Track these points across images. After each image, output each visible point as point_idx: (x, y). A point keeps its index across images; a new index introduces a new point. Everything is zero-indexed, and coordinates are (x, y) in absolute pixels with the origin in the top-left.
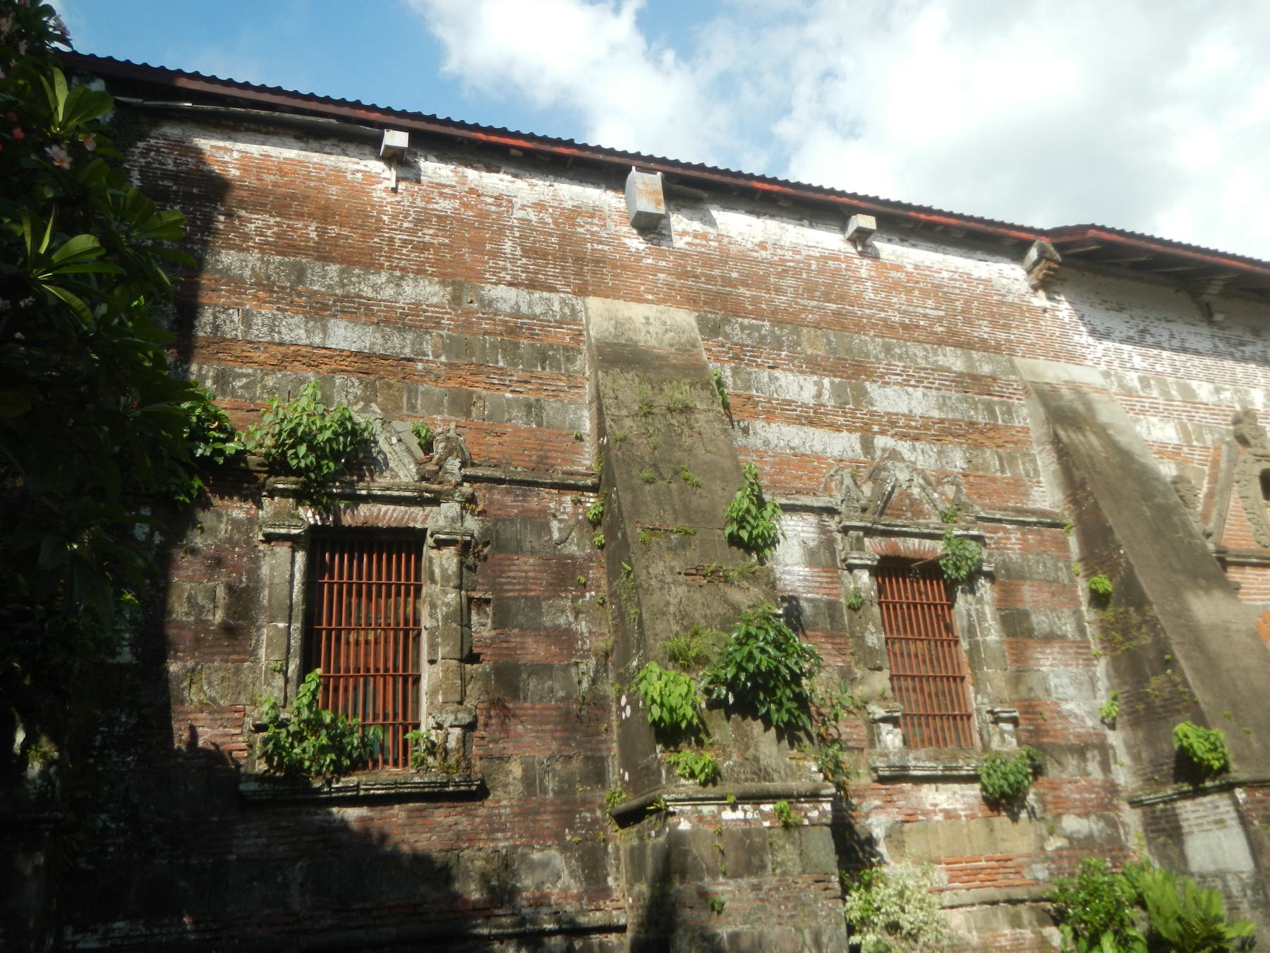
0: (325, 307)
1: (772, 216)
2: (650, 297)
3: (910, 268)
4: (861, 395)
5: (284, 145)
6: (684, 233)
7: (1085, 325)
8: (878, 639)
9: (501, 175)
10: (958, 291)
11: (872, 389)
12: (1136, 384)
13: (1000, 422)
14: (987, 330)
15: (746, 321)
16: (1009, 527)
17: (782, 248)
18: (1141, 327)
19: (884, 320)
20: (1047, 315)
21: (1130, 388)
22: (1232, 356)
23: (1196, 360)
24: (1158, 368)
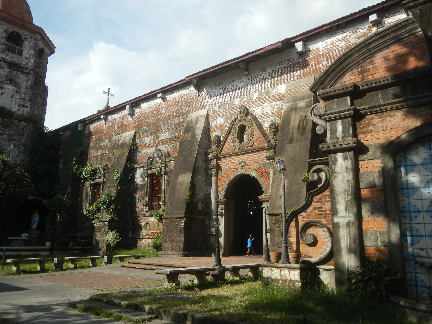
1: (150, 101)
3: (172, 100)
4: (157, 137)
6: (137, 112)
8: (147, 191)
9: (116, 114)
10: (180, 101)
11: (159, 135)
12: (217, 108)
14: (184, 109)
15: (142, 128)
18: (224, 88)
19: (165, 117)
21: (215, 111)
22: (252, 84)
23: (238, 91)
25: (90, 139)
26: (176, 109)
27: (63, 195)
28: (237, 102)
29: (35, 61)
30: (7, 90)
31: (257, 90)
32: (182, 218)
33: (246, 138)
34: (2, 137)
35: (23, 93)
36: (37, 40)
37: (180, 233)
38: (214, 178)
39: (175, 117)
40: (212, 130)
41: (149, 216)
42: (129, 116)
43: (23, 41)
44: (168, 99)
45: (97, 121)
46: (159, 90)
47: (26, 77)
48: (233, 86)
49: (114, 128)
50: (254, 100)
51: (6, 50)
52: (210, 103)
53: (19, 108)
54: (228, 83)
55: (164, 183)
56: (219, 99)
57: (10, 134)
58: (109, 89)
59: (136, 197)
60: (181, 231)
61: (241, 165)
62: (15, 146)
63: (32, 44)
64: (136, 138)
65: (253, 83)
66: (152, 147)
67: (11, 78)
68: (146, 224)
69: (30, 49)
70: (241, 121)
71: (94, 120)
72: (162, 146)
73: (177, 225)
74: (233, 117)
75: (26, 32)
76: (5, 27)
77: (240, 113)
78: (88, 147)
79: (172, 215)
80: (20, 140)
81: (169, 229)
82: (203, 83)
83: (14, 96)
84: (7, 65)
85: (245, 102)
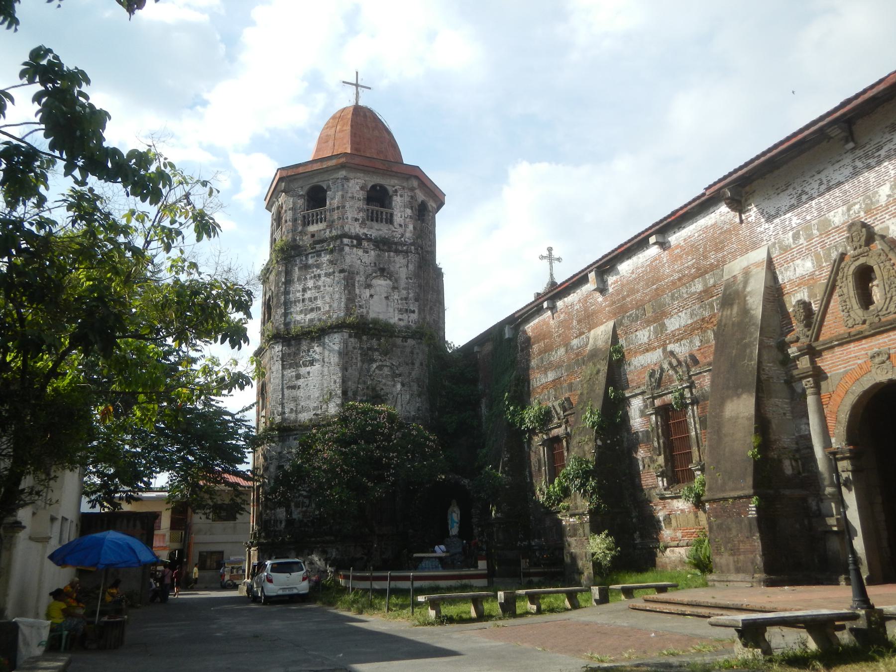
0: (546, 368)
1: (634, 255)
2: (604, 320)
3: (682, 243)
4: (663, 326)
5: (536, 318)
6: (612, 284)
7: (764, 217)
8: (659, 443)
9: (572, 295)
10: (701, 242)
11: (667, 321)
12: (791, 240)
13: (716, 311)
14: (713, 257)
15: (628, 314)
16: (705, 374)
17: (638, 268)
18: (800, 192)
19: (672, 281)
20: (743, 225)
21: (787, 246)
22: (869, 167)
23: (837, 192)
24: (808, 218)
25: (529, 352)
26: (694, 260)
27: (496, 467)
28: (838, 217)
29: (414, 228)
30: (378, 289)
31: (886, 178)
32: (749, 497)
33: (877, 294)
34: (381, 372)
35: (403, 289)
36: (412, 189)
37: (750, 532)
38: (811, 400)
39: (695, 278)
40: (785, 291)
41: (672, 498)
42: (598, 294)
43: (391, 197)
44: (672, 244)
45: (537, 316)
46: (650, 228)
47: (404, 258)
48: (821, 184)
49: (572, 323)
50: (884, 204)
51: (368, 220)
52: (770, 233)
53: (401, 317)
54: (807, 179)
55: (695, 424)
56: (791, 220)
57: (393, 364)
58: (550, 250)
59: (637, 460)
60: (751, 527)
61: (877, 360)
62: (403, 385)
63: (407, 199)
64: (619, 336)
65: (873, 164)
66: (655, 349)
67: (381, 266)
68: (669, 515)
69: (405, 207)
70: (856, 258)
71: (532, 313)
72: (677, 344)
73: (739, 514)
74: (836, 253)
75: (394, 181)
76: (361, 182)
77: (850, 239)
78: (528, 368)
79: (724, 491)
80: (410, 374)
81: (722, 524)
82: (747, 193)
83: (390, 296)
84: (373, 245)
85: (859, 212)
